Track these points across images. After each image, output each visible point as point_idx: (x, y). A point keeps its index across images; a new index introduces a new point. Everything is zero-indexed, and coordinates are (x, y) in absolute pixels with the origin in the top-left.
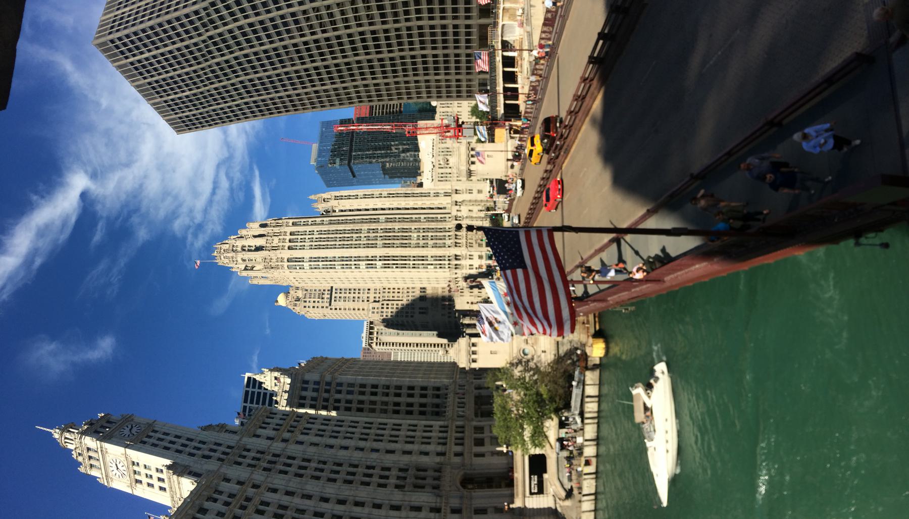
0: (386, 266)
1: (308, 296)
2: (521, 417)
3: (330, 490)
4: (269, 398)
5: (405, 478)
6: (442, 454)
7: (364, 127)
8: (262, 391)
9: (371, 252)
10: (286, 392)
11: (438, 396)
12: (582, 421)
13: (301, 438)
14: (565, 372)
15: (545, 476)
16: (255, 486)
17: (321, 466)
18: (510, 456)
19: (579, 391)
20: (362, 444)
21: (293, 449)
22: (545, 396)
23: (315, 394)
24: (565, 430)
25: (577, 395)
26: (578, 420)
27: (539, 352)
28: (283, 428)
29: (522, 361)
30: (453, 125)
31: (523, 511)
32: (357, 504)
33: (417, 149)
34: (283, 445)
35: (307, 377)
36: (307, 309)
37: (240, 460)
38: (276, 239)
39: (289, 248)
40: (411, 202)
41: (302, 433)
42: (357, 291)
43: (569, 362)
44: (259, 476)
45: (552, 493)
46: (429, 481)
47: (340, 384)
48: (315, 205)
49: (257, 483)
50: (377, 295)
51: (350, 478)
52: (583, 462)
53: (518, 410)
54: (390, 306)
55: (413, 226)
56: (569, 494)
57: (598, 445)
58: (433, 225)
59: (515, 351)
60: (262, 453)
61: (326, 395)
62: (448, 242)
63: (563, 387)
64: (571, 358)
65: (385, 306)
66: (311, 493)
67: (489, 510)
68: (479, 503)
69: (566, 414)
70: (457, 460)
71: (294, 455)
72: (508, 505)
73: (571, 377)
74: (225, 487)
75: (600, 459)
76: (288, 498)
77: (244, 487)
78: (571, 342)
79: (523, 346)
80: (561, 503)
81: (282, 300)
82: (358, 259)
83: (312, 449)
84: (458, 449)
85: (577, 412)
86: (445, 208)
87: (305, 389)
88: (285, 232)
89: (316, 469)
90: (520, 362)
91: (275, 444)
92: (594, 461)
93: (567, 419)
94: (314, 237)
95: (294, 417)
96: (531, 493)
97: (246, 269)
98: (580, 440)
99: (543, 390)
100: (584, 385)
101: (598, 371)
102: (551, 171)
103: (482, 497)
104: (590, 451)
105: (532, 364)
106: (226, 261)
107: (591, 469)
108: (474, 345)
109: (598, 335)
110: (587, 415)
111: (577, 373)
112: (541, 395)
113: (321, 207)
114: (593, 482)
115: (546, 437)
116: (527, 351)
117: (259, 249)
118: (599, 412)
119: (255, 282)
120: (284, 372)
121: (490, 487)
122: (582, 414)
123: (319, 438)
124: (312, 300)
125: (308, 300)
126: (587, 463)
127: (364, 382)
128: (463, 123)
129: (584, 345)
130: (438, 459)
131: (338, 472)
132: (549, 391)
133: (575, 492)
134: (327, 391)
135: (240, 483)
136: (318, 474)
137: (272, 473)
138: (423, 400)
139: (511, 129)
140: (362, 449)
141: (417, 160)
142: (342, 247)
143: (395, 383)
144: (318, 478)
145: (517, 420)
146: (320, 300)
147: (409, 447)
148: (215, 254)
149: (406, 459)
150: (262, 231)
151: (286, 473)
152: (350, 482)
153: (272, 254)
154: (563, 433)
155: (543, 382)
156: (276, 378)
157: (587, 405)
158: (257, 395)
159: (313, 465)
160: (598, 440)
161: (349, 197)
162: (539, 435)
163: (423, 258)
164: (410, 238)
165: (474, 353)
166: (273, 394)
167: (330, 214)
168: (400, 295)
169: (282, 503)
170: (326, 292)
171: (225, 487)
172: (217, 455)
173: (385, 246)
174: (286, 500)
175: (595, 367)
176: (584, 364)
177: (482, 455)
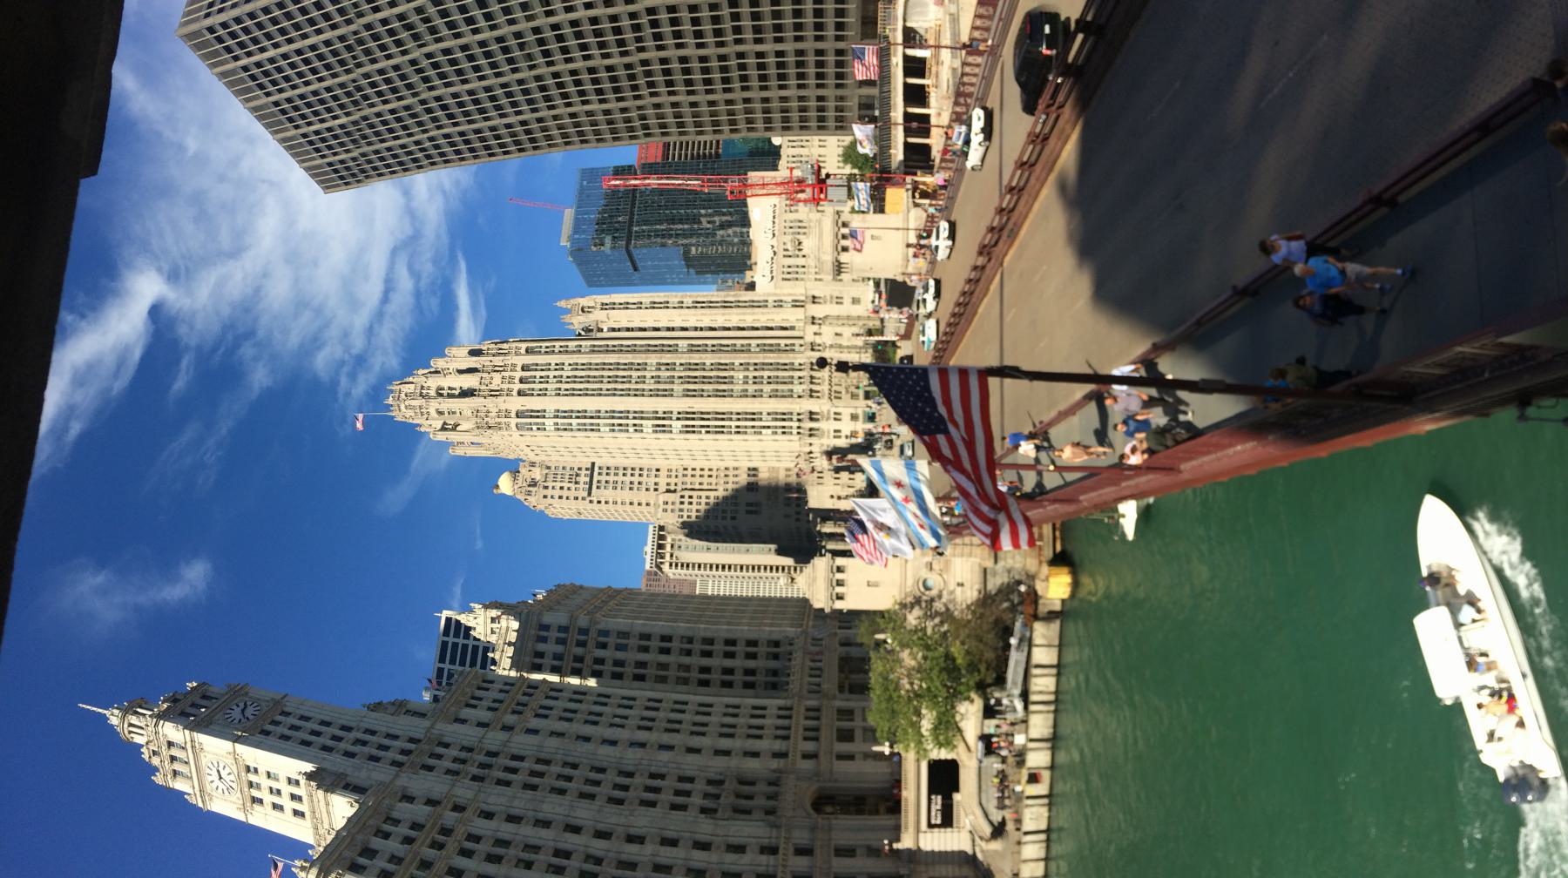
0: (689, 430)
1: (551, 477)
2: (917, 696)
3: (585, 813)
4: (480, 654)
5: (717, 797)
6: (782, 755)
7: (653, 182)
8: (471, 643)
9: (662, 404)
10: (510, 644)
11: (776, 657)
12: (1026, 708)
13: (535, 723)
14: (997, 621)
15: (957, 797)
16: (457, 808)
17: (568, 771)
18: (895, 760)
19: (1022, 657)
20: (642, 736)
21: (522, 743)
22: (959, 661)
23: (560, 649)
24: (994, 722)
25: (1017, 662)
26: (1019, 705)
27: (952, 586)
28: (504, 705)
29: (922, 600)
30: (811, 180)
31: (915, 856)
32: (631, 839)
33: (745, 222)
34: (503, 736)
35: (548, 618)
36: (549, 500)
37: (431, 762)
38: (497, 378)
39: (520, 393)
40: (734, 318)
41: (537, 716)
42: (637, 472)
43: (1006, 605)
44: (464, 791)
45: (968, 827)
46: (760, 801)
47: (605, 633)
48: (567, 318)
49: (461, 802)
50: (673, 480)
51: (618, 794)
52: (1025, 778)
53: (912, 684)
54: (694, 500)
55: (738, 359)
56: (998, 831)
57: (1053, 749)
58: (771, 358)
59: (910, 582)
60: (470, 750)
61: (579, 651)
62: (798, 389)
63: (996, 649)
64: (1008, 600)
65: (686, 500)
66: (549, 817)
67: (858, 852)
68: (843, 838)
69: (997, 695)
70: (807, 765)
71: (522, 753)
72: (890, 844)
73: (1008, 631)
75: (1057, 773)
76: (511, 827)
77: (438, 809)
78: (1009, 571)
79: (924, 574)
80: (983, 844)
81: (505, 484)
82: (640, 415)
83: (553, 742)
84: (810, 746)
85: (1017, 691)
86: (793, 328)
87: (544, 640)
88: (514, 365)
89: (559, 777)
90: (918, 601)
91: (491, 734)
92: (1046, 775)
93: (999, 702)
94: (565, 374)
95: (524, 688)
96: (930, 826)
97: (443, 429)
98: (1020, 740)
99: (957, 650)
100: (1030, 646)
101: (1058, 622)
102: (983, 268)
103: (847, 828)
104: (1038, 759)
105: (938, 606)
106: (410, 413)
107: (1042, 789)
108: (840, 570)
109: (1060, 560)
110: (1033, 698)
111: (1018, 625)
112: (954, 660)
113: (578, 322)
114: (1044, 812)
115: (960, 730)
116: (930, 583)
117: (467, 393)
118: (1057, 693)
119: (460, 452)
120: (509, 609)
121: (860, 812)
122: (1025, 695)
123: (566, 725)
124: (558, 485)
125: (550, 484)
126: (1034, 778)
127: (647, 630)
128: (828, 176)
129: (1032, 577)
130: (775, 764)
131: (597, 783)
132: (968, 652)
133: (1010, 826)
134: (582, 644)
135: (430, 802)
136: (562, 784)
137: (486, 784)
138: (751, 664)
139: (915, 189)
140: (643, 745)
141: (746, 243)
142: (613, 393)
143: (702, 634)
144: (562, 792)
145: (910, 700)
146: (573, 486)
147: (725, 743)
148: (390, 401)
149: (720, 763)
151: (508, 784)
152: (620, 802)
153: (491, 403)
154: (990, 726)
155: (957, 637)
156: (493, 620)
157: (1034, 681)
158: (462, 650)
159: (556, 769)
160: (1054, 741)
161: (626, 306)
162: (947, 728)
163: (753, 416)
164: (731, 381)
165: (840, 583)
166: (489, 648)
167: (594, 335)
168: (713, 480)
169: (501, 835)
170: (583, 472)
172: (390, 755)
173: (688, 394)
174: (507, 830)
175: (1051, 616)
176: (1031, 611)
177: (851, 757)
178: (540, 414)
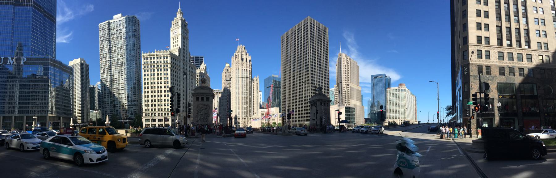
0: (236, 98)
4: (198, 66)
9: (240, 93)
40: (255, 105)
44: (182, 70)
55: (248, 106)
74: (179, 62)
81: (227, 65)
82: (239, 89)
113: (255, 79)
117: (242, 60)
120: (205, 70)
142: (242, 85)
150: (248, 61)
158: (198, 61)
161: (257, 87)
163: (239, 108)
171: (179, 62)
173: (242, 98)
178: (238, 72)
